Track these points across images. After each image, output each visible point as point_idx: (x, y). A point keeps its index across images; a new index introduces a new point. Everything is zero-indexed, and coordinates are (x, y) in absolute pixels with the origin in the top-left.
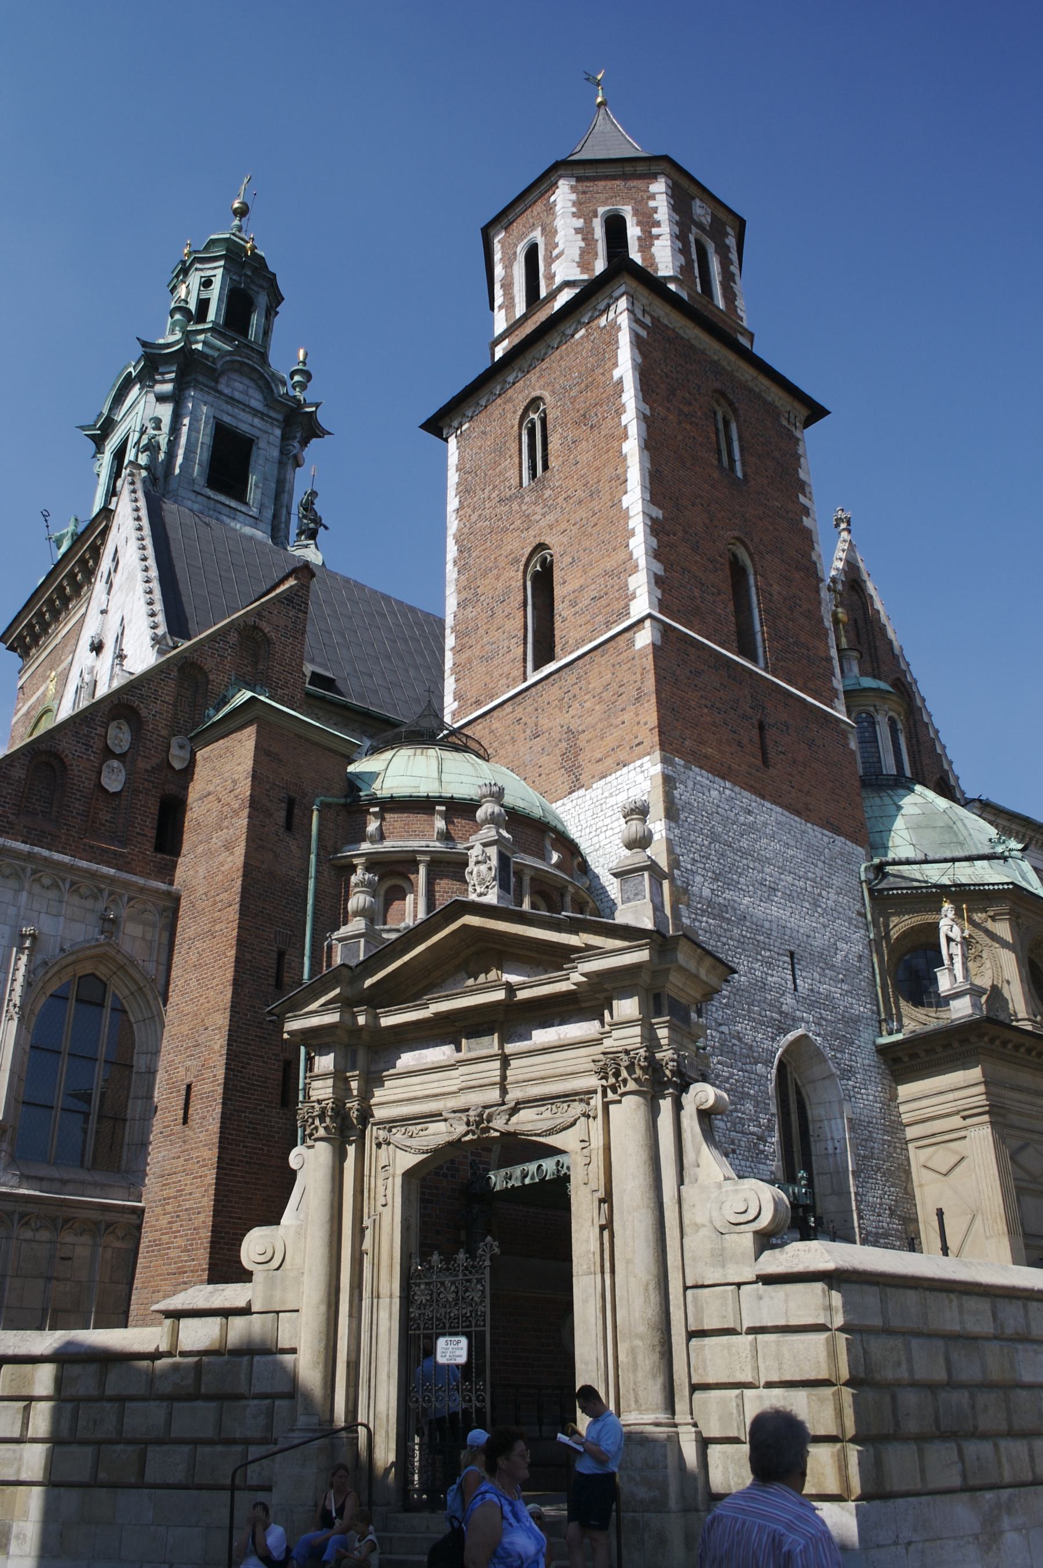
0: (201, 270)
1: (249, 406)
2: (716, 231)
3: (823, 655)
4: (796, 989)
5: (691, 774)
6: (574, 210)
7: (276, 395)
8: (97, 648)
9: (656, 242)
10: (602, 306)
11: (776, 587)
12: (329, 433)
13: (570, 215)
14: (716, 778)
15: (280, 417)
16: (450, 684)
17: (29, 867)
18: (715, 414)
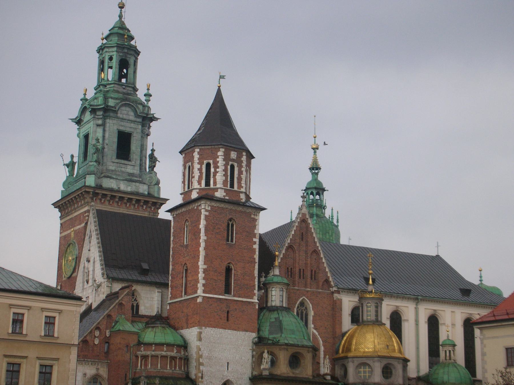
0: (109, 52)
1: (129, 120)
2: (239, 156)
3: (252, 285)
5: (206, 329)
6: (198, 161)
7: (138, 113)
8: (89, 261)
9: (218, 174)
10: (199, 204)
12: (159, 119)
13: (197, 163)
14: (214, 329)
15: (140, 120)
16: (170, 288)
17: (84, 362)
18: (228, 224)
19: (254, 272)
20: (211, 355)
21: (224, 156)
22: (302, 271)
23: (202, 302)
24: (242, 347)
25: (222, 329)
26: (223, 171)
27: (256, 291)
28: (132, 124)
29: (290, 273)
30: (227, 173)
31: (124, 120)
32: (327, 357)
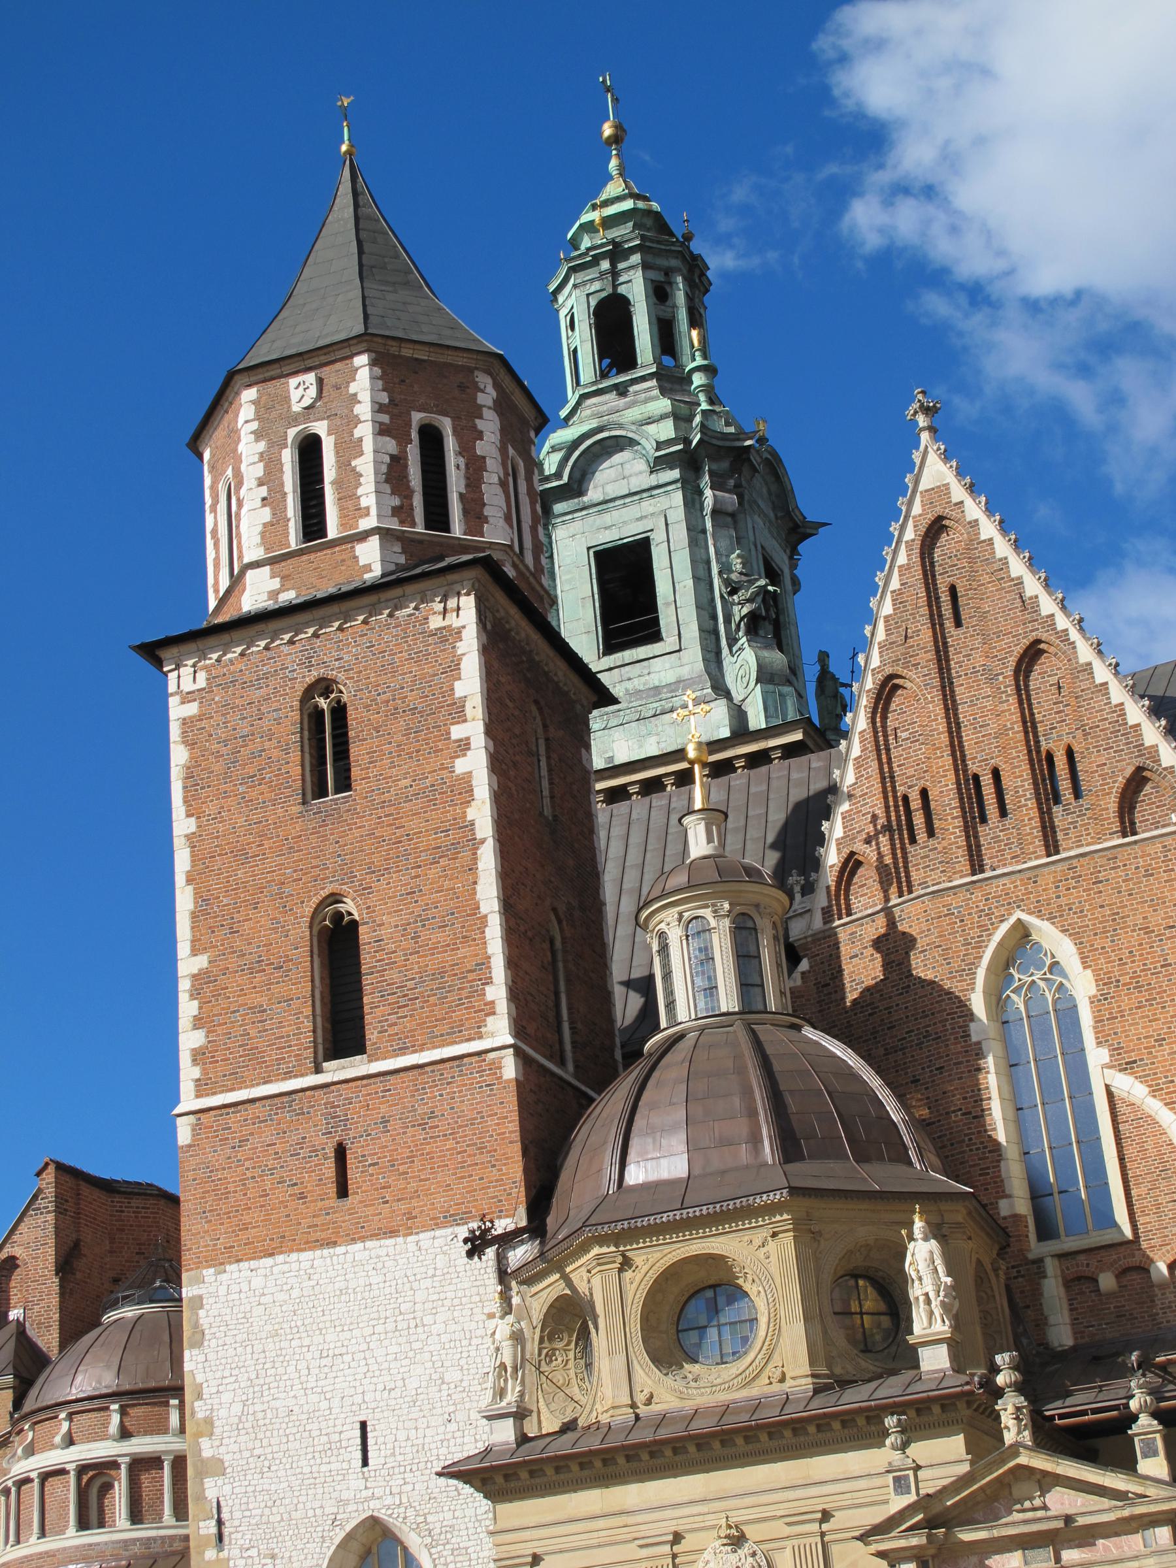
4: (365, 1463)
5: (224, 1277)
9: (244, 511)
11: (393, 920)
19: (475, 893)
20: (258, 1407)
21: (258, 417)
22: (987, 781)
23: (189, 1146)
24: (440, 1318)
25: (310, 1249)
26: (260, 484)
27: (498, 992)
28: (644, 504)
29: (919, 820)
30: (282, 485)
31: (611, 505)
32: (918, 1225)
